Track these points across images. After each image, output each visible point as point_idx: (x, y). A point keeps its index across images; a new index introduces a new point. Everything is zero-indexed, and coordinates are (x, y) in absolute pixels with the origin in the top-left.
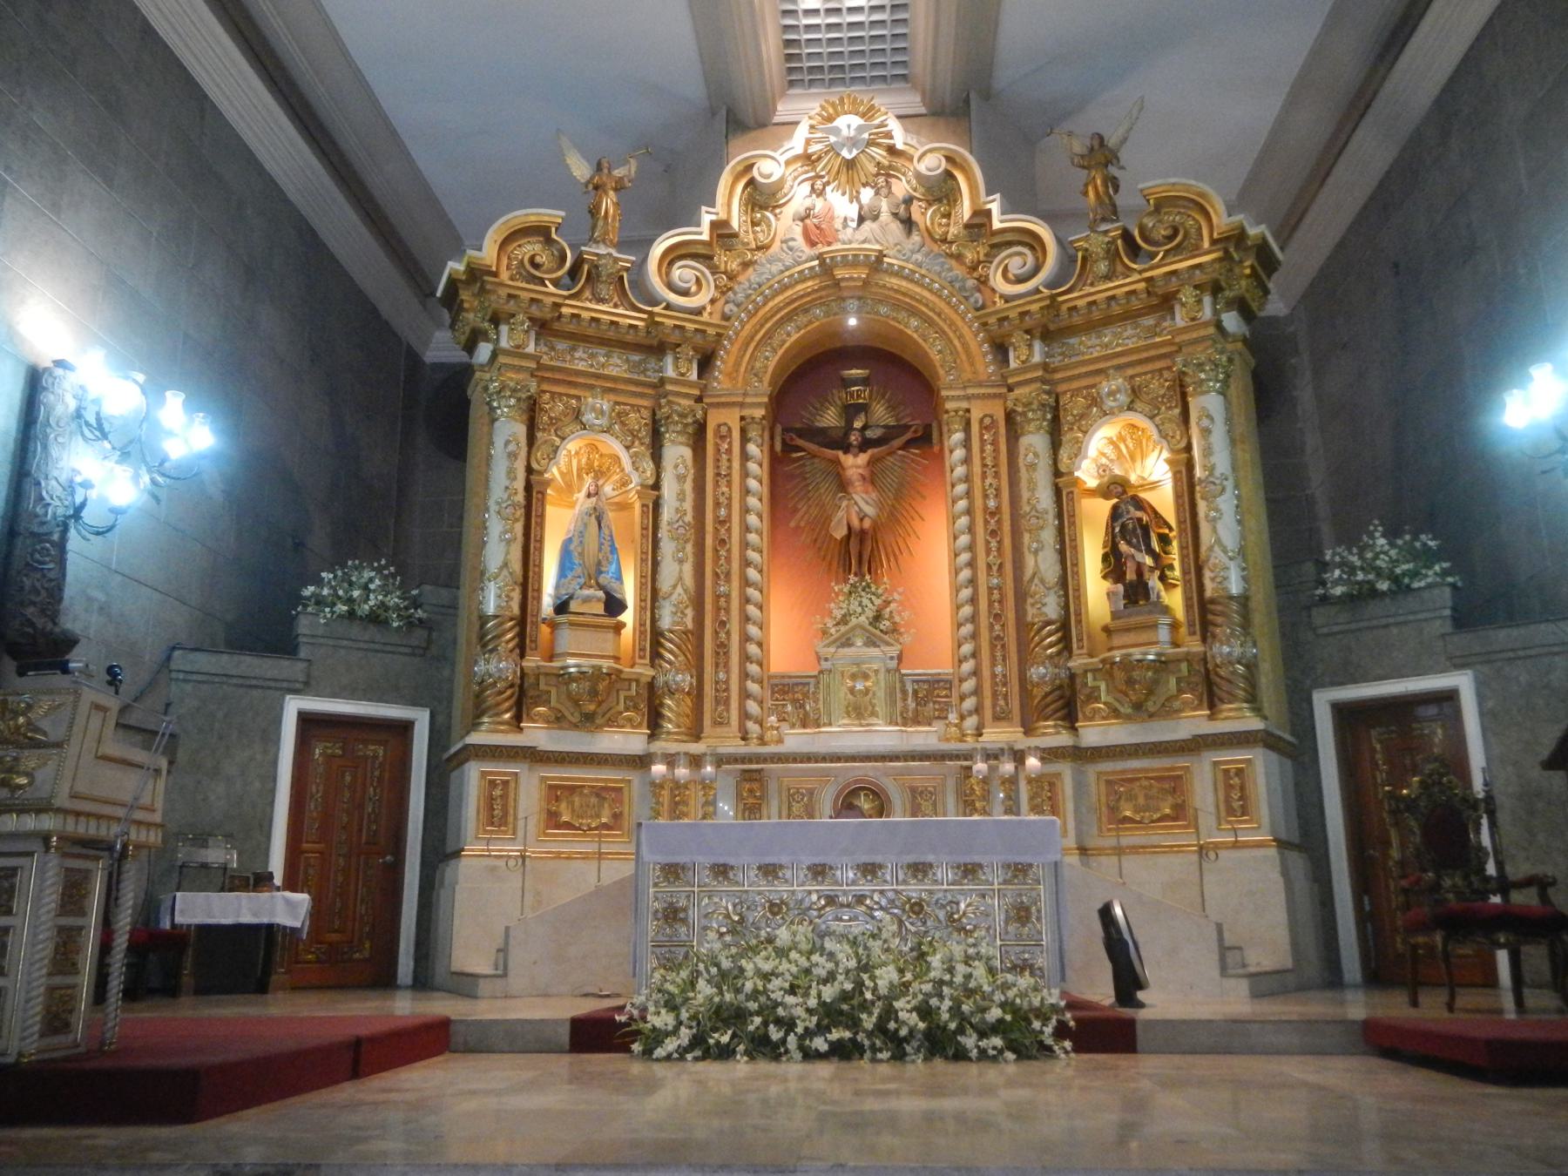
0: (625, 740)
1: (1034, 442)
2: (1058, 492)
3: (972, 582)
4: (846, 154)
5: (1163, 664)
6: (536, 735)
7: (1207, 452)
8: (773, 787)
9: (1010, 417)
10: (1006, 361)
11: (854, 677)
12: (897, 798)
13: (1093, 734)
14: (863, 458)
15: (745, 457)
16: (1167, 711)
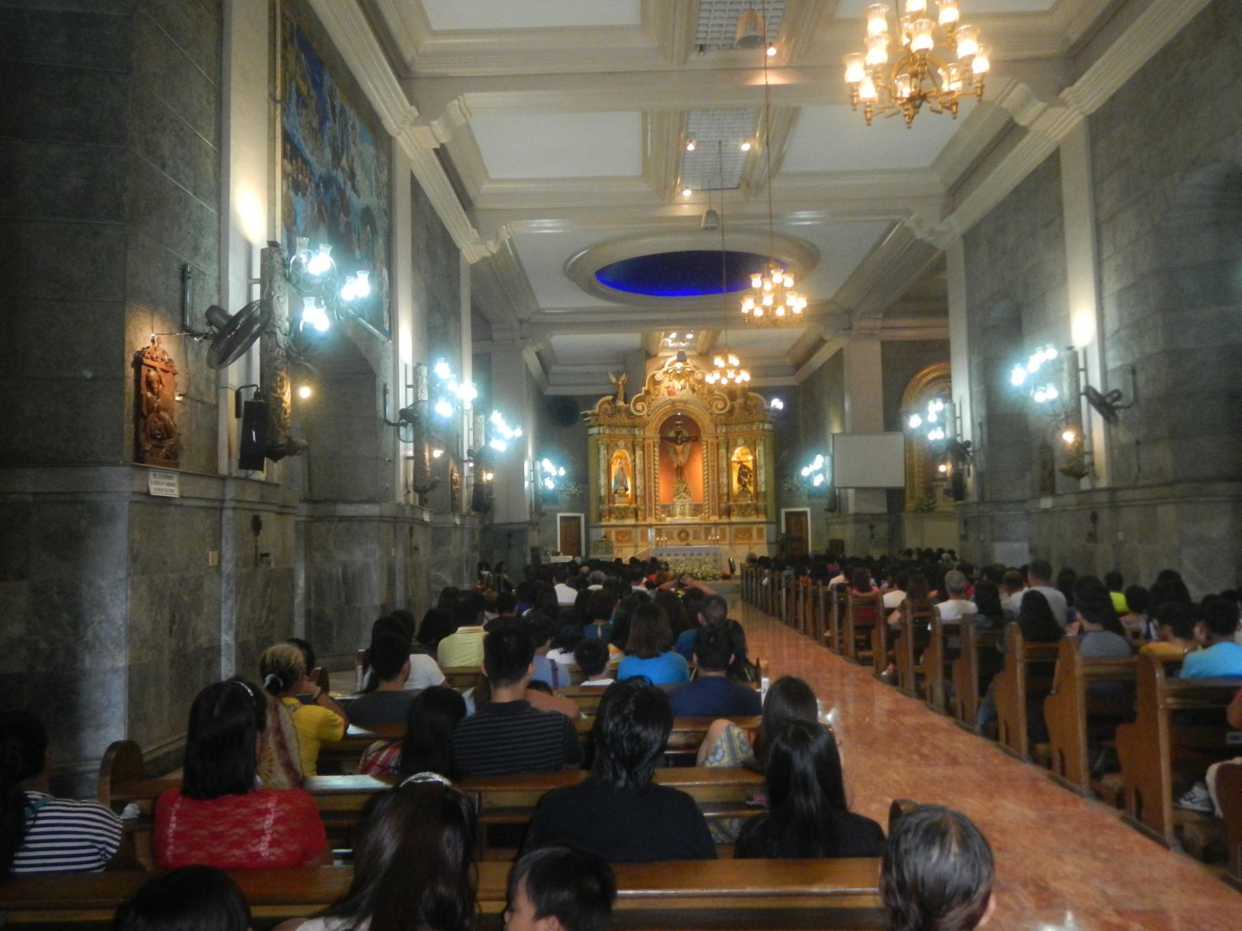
0: (631, 521)
1: (723, 451)
2: (728, 465)
3: (708, 482)
4: (678, 372)
5: (748, 505)
6: (613, 522)
7: (759, 459)
8: (663, 531)
9: (718, 444)
10: (716, 431)
11: (683, 506)
12: (691, 534)
13: (734, 519)
14: (681, 446)
15: (654, 451)
16: (749, 515)
